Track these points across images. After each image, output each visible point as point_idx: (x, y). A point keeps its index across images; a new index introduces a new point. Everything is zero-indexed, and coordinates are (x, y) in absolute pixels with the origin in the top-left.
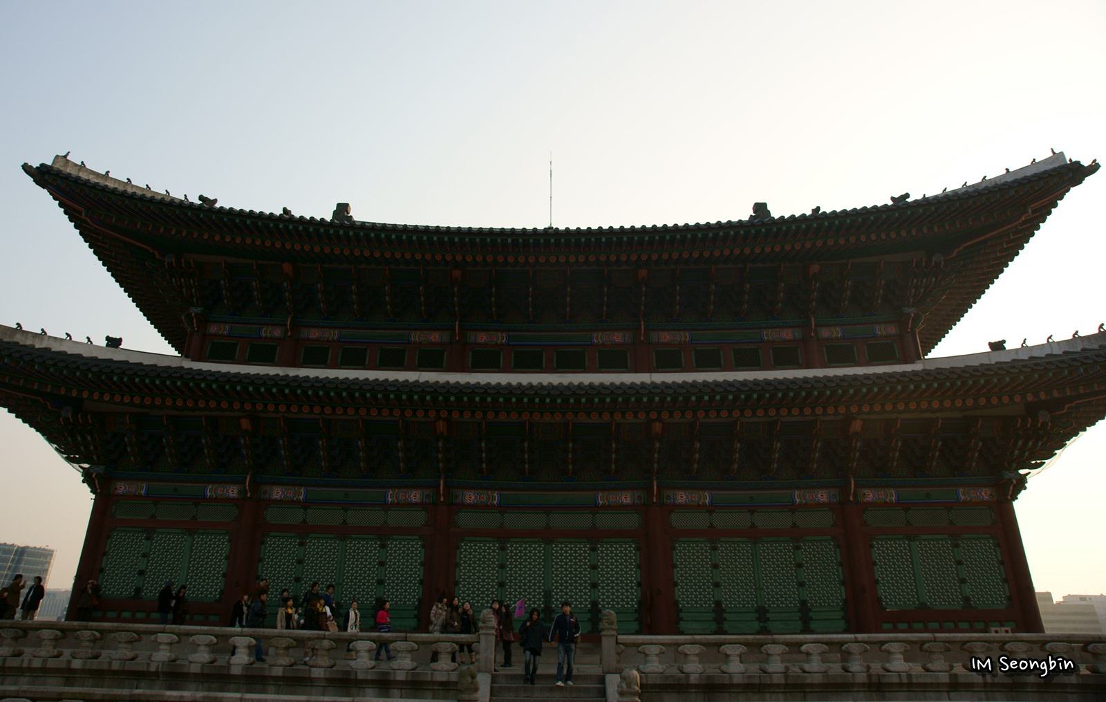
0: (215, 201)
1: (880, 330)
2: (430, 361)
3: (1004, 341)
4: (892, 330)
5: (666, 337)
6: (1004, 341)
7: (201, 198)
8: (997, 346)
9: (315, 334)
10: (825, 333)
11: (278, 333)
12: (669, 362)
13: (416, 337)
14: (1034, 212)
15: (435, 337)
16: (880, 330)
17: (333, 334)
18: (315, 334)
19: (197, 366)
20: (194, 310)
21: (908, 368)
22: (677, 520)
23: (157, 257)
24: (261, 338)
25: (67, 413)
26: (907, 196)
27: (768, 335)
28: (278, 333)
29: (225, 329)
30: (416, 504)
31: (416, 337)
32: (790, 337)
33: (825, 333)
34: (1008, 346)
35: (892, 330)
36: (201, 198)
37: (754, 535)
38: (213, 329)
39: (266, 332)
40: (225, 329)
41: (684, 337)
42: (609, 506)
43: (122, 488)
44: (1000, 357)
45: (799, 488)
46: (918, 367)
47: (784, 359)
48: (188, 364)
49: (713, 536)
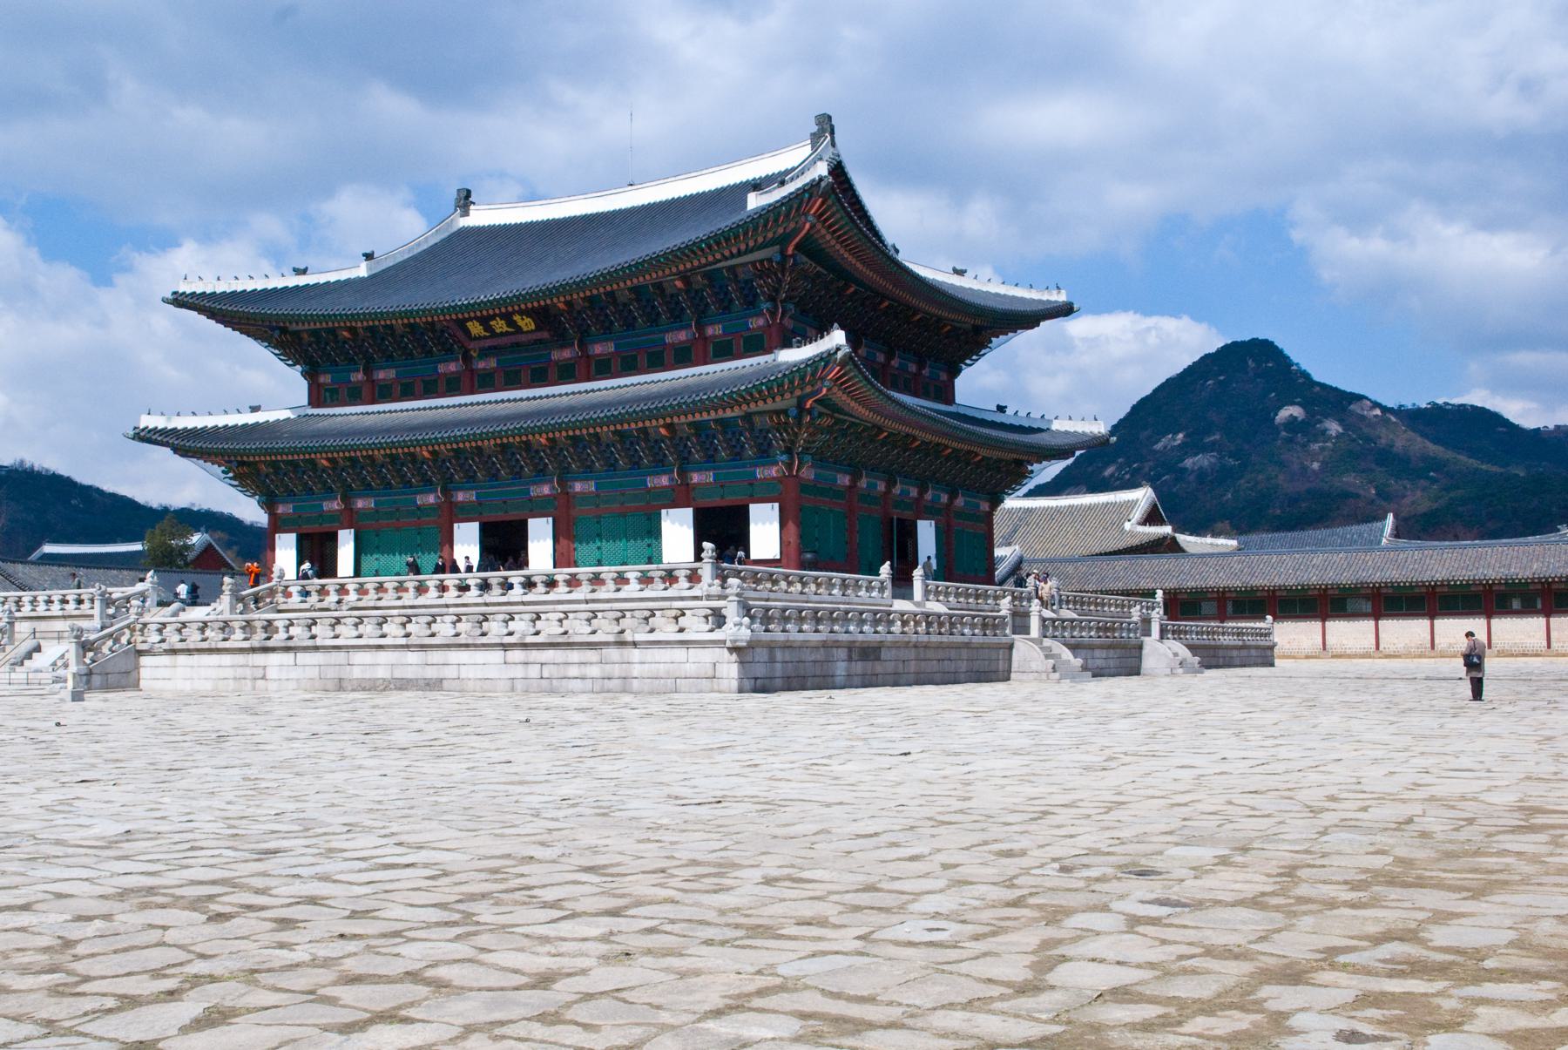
10: (710, 331)
17: (392, 374)
35: (761, 322)
48: (311, 411)
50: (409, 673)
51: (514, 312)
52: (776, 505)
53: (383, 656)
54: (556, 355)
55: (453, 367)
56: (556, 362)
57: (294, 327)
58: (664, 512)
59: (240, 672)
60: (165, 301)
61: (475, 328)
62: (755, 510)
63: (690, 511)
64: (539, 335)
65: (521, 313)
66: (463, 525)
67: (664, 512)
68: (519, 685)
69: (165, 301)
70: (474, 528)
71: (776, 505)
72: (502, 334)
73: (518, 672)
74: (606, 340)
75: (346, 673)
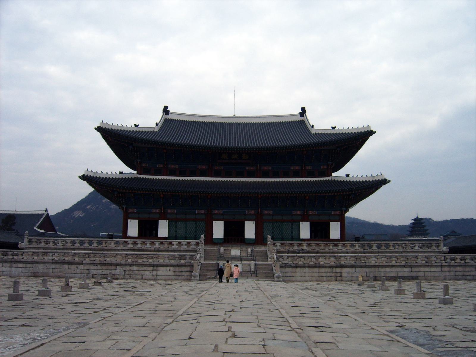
0: (138, 125)
1: (322, 167)
3: (349, 175)
4: (325, 167)
5: (265, 168)
6: (349, 175)
7: (135, 125)
8: (348, 176)
9: (172, 166)
10: (307, 168)
11: (162, 166)
13: (199, 167)
14: (361, 140)
15: (204, 167)
16: (322, 167)
17: (177, 167)
18: (172, 166)
19: (142, 176)
20: (139, 161)
21: (327, 179)
22: (264, 217)
23: (127, 146)
25: (116, 193)
26: (335, 127)
27: (292, 168)
28: (162, 166)
29: (147, 165)
31: (199, 167)
33: (307, 168)
34: (350, 176)
35: (325, 167)
36: (135, 125)
38: (143, 165)
39: (159, 166)
40: (147, 165)
41: (270, 168)
43: (130, 210)
44: (348, 179)
45: (294, 210)
46: (330, 178)
48: (139, 176)
50: (405, 274)
52: (339, 223)
53: (394, 269)
54: (247, 168)
55: (204, 167)
58: (301, 222)
59: (329, 274)
60: (95, 129)
63: (309, 223)
67: (301, 222)
68: (447, 278)
69: (95, 129)
70: (222, 223)
71: (339, 223)
73: (447, 274)
75: (377, 274)
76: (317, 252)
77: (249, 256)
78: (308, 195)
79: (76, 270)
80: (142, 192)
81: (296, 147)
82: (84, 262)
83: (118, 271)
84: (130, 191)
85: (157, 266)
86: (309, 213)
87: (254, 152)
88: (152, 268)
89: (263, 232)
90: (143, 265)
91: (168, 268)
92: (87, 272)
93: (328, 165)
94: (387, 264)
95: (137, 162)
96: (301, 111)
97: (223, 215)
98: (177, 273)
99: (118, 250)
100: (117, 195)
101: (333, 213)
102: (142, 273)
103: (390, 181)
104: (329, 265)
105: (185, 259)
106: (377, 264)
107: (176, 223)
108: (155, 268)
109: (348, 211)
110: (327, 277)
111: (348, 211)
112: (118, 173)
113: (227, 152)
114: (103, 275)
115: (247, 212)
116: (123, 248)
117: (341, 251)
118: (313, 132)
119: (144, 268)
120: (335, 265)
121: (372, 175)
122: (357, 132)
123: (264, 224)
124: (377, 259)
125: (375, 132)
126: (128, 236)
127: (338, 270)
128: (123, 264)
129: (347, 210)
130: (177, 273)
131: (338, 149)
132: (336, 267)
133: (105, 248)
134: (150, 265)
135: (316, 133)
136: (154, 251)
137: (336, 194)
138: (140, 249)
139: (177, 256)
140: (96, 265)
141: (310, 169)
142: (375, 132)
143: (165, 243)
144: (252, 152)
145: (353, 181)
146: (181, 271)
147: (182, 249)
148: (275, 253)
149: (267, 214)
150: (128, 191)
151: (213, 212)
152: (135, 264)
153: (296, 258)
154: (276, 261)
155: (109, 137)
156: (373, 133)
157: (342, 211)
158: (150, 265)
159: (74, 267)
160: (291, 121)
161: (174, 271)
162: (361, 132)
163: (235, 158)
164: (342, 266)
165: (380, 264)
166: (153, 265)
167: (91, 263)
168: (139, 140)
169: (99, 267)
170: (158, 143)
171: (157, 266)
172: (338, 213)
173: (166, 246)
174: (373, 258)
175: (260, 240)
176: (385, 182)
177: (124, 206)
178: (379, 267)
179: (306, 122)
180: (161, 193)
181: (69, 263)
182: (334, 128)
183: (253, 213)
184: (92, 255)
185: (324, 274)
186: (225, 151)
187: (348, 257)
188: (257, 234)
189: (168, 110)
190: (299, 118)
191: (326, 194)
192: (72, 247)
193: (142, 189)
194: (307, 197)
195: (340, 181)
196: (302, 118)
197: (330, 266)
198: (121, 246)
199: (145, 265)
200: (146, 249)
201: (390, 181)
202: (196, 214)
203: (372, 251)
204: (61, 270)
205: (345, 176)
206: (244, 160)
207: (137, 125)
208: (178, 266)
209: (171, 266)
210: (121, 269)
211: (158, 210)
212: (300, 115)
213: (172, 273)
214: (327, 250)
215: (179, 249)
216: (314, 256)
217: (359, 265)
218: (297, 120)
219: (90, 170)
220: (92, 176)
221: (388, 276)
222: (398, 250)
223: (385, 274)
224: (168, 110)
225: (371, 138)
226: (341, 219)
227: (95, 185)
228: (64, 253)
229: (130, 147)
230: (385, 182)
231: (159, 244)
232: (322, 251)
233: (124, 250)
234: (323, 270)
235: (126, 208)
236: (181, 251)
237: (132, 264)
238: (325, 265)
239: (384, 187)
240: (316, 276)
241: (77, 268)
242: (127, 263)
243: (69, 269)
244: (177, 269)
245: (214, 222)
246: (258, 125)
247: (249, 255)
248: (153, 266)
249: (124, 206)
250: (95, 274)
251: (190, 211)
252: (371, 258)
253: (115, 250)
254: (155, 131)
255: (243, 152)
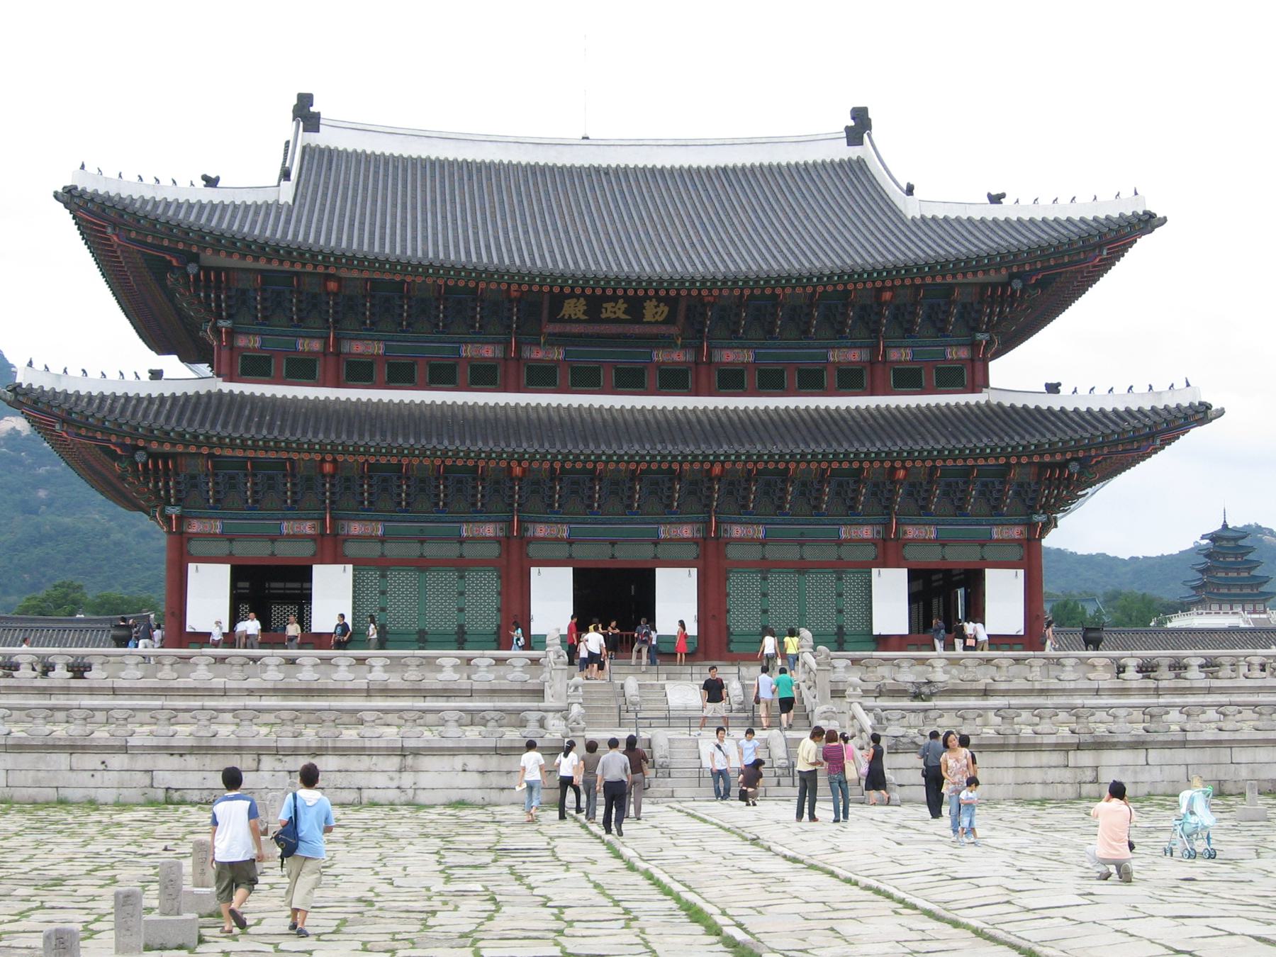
0: (217, 179)
2: (484, 378)
3: (1059, 384)
4: (964, 353)
6: (1059, 384)
7: (205, 178)
8: (1053, 388)
9: (356, 348)
10: (894, 355)
11: (316, 346)
12: (731, 382)
13: (468, 351)
15: (489, 352)
17: (377, 348)
19: (237, 388)
23: (175, 263)
24: (296, 351)
26: (1003, 196)
28: (316, 346)
29: (253, 342)
30: (490, 538)
31: (468, 351)
32: (857, 359)
33: (894, 355)
35: (964, 353)
36: (205, 178)
37: (802, 567)
38: (241, 342)
40: (253, 342)
41: (747, 356)
42: (671, 540)
43: (196, 527)
44: (1054, 402)
47: (850, 382)
48: (226, 387)
49: (765, 567)
51: (647, 297)
52: (1021, 572)
54: (660, 356)
55: (489, 352)
56: (659, 365)
57: (208, 258)
58: (875, 571)
61: (574, 308)
62: (993, 578)
63: (906, 570)
64: (663, 330)
65: (667, 300)
66: (545, 570)
67: (875, 571)
69: (56, 195)
70: (567, 574)
72: (608, 321)
74: (743, 348)
76: (986, 693)
77: (739, 711)
78: (909, 464)
79: (98, 775)
80: (250, 454)
81: (860, 275)
82: (133, 741)
83: (267, 775)
84: (193, 449)
85: (417, 752)
86: (905, 533)
87: (694, 293)
88: (395, 762)
89: (728, 611)
90: (364, 748)
91: (458, 761)
92: (146, 780)
93: (974, 345)
94: (1260, 735)
95: (217, 331)
96: (852, 123)
97: (570, 542)
98: (494, 780)
99: (225, 693)
100: (145, 465)
101: (997, 533)
102: (360, 779)
103: (1221, 413)
104: (1052, 739)
105: (523, 724)
106: (1224, 736)
107: (383, 576)
108: (410, 760)
109: (1056, 526)
110: (1044, 783)
111: (1056, 526)
112: (145, 376)
113: (588, 292)
114: (206, 793)
115: (664, 532)
116: (246, 685)
117: (1072, 685)
118: (911, 209)
119: (366, 762)
120: (1075, 739)
121: (1151, 387)
122: (1090, 217)
123: (727, 579)
124: (1225, 715)
125: (1164, 221)
126: (188, 630)
127: (1086, 758)
128: (284, 748)
129: (1050, 524)
130: (494, 780)
131: (1017, 284)
132: (1079, 747)
133: (175, 684)
134: (390, 751)
135: (923, 218)
136: (369, 693)
137: (1013, 460)
138: (315, 686)
139: (493, 714)
140: (182, 752)
141: (906, 361)
142: (1164, 221)
143: (408, 661)
144: (683, 293)
145: (1076, 411)
146: (509, 772)
147: (476, 686)
148: (857, 696)
149: (740, 540)
150: (180, 449)
151: (530, 534)
152: (335, 748)
153: (932, 714)
154: (873, 729)
155: (109, 230)
156: (1154, 221)
157: (1031, 526)
158: (390, 751)
159: (92, 761)
160: (811, 162)
161: (482, 772)
162: (1107, 218)
163: (613, 316)
164: (1099, 745)
165: (1238, 736)
166: (402, 748)
167: (158, 748)
168: (204, 238)
169: (191, 761)
170: (314, 256)
171: (417, 752)
172: (1015, 532)
173: (413, 674)
174: (1211, 714)
175: (715, 641)
176: (1200, 414)
177: (173, 511)
178: (1231, 744)
179: (875, 167)
180: (329, 458)
181: (72, 748)
182: (996, 199)
183: (685, 536)
184: (163, 715)
185: (1035, 775)
186: (578, 291)
187: (1122, 712)
188: (703, 618)
189: (312, 109)
190: (842, 151)
191: (976, 460)
192: (41, 682)
193: (196, 437)
194: (901, 473)
195: (1012, 406)
196: (854, 152)
197: (1056, 745)
198: (237, 675)
199: (371, 749)
200: (339, 686)
201: (1221, 413)
202: (462, 541)
203: (1187, 684)
204: (41, 774)
205: (1044, 389)
206: (649, 323)
207: (213, 176)
208: (497, 751)
209: (471, 750)
210: (279, 766)
211: (309, 524)
212: (847, 137)
213: (475, 779)
214: (1019, 684)
215: (465, 684)
216: (999, 709)
217: (1161, 738)
218: (837, 160)
219: (38, 365)
220: (46, 389)
221: (1263, 777)
222: (1249, 683)
223: (1253, 771)
224: (312, 109)
225: (1144, 245)
226: (1028, 558)
227: (57, 427)
228: (50, 709)
229: (192, 269)
230: (1200, 414)
231: (384, 666)
232: (1003, 686)
233: (251, 692)
234: (1031, 759)
235: (180, 518)
236: (471, 693)
237: (320, 748)
238: (1039, 741)
239: (1196, 433)
240: (1006, 781)
241: (103, 767)
242: (302, 742)
243: (71, 769)
244: (493, 762)
245: (534, 570)
246: (681, 175)
247: (735, 706)
248: (403, 752)
249: (173, 511)
250: (177, 790)
251: (446, 527)
252: (1204, 712)
253: (210, 692)
254: (281, 202)
255: (651, 293)
